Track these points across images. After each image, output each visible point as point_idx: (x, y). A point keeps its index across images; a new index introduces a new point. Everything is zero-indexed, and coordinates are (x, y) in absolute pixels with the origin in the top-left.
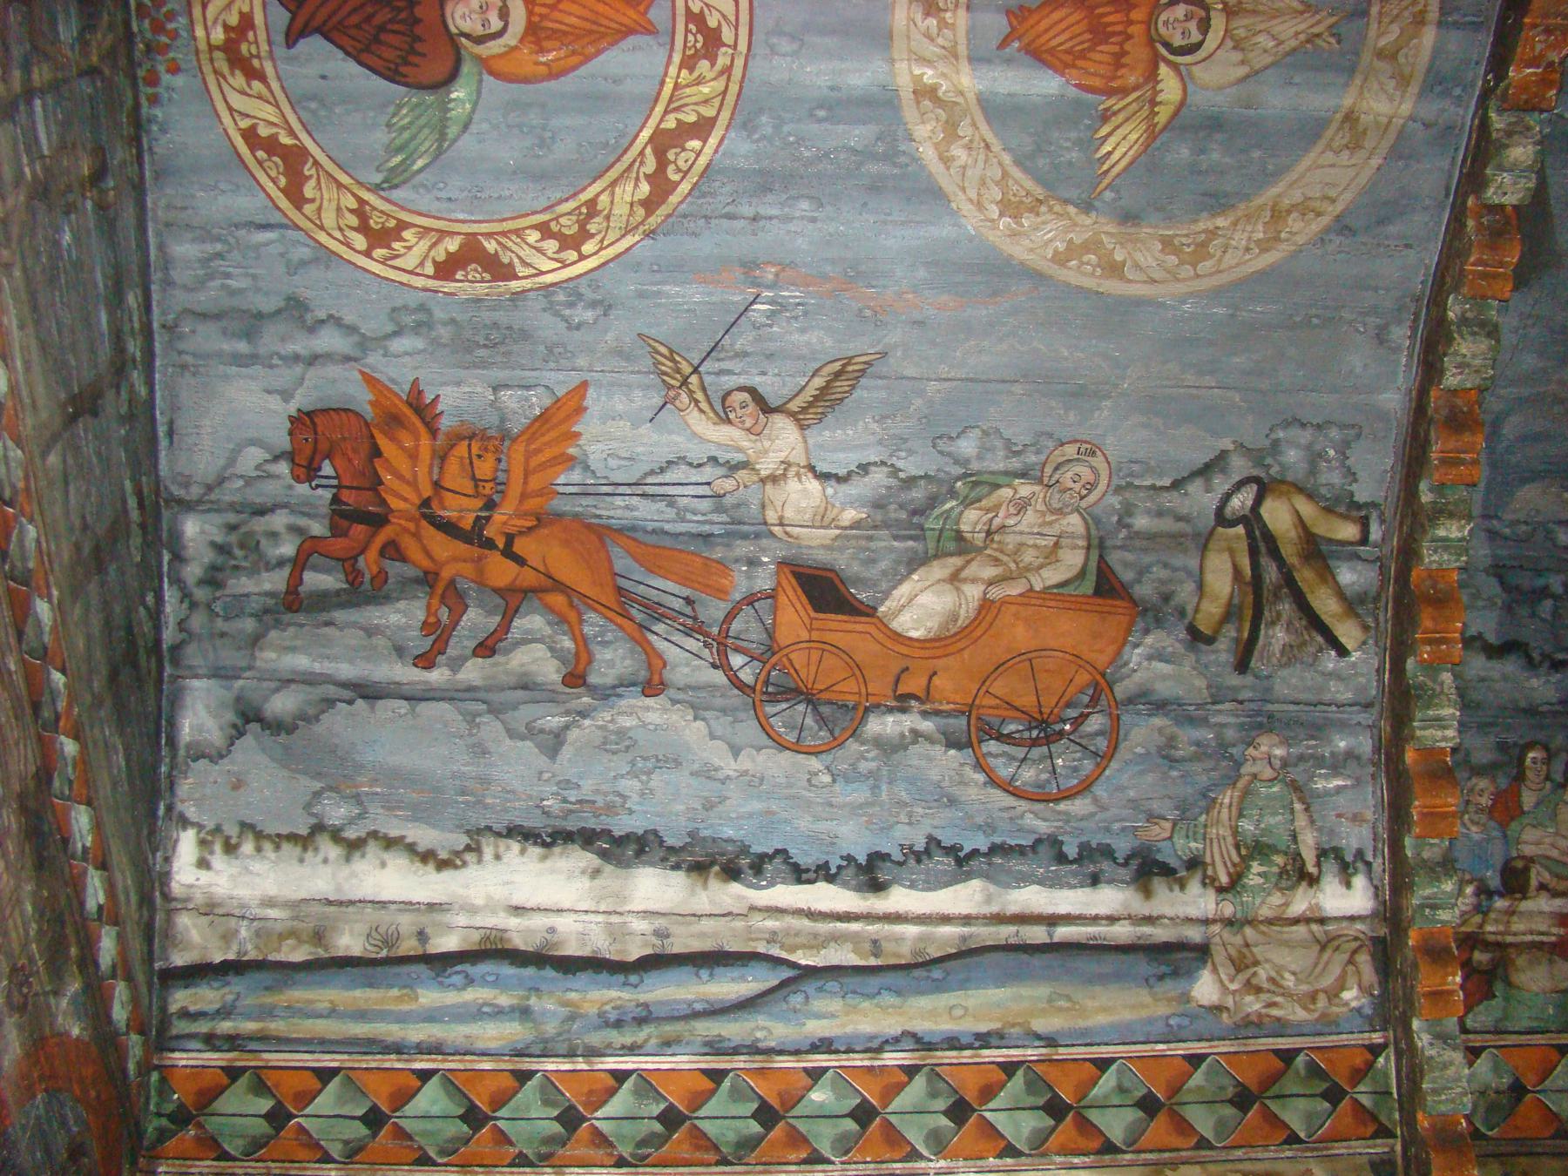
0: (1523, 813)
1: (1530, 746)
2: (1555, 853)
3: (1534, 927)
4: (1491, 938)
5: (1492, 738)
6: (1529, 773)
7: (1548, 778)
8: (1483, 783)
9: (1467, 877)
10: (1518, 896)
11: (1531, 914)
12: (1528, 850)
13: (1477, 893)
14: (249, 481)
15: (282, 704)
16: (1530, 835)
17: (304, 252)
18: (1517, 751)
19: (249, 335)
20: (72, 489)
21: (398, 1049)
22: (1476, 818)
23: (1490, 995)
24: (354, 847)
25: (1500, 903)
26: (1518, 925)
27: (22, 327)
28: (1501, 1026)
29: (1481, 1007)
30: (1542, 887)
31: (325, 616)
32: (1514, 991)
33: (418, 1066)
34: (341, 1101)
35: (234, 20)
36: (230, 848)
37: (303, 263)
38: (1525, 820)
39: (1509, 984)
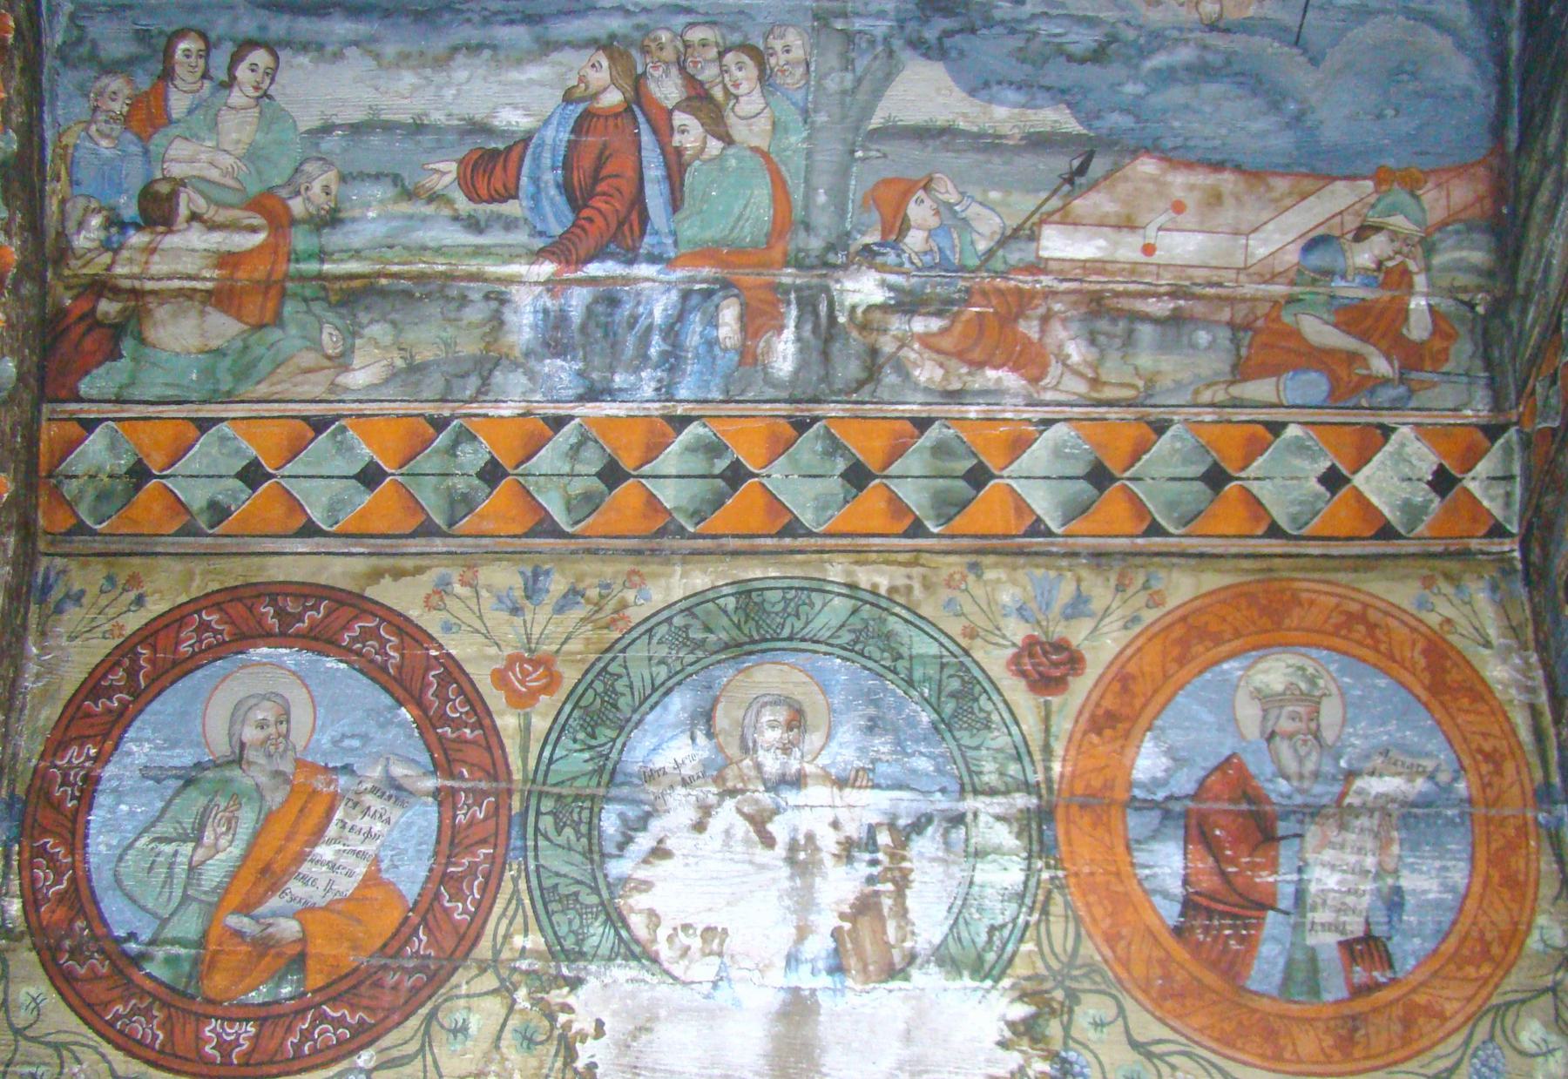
0: (170, 122)
1: (181, 34)
2: (214, 174)
3: (180, 268)
4: (126, 284)
5: (129, 27)
6: (179, 70)
7: (205, 75)
8: (116, 84)
9: (94, 205)
10: (161, 229)
11: (177, 252)
12: (177, 170)
13: (109, 223)
16: (180, 149)
18: (162, 42)
22: (106, 128)
23: (115, 355)
25: (137, 239)
26: (159, 266)
28: (126, 395)
29: (101, 370)
30: (194, 217)
32: (147, 351)
38: (174, 131)
39: (143, 341)
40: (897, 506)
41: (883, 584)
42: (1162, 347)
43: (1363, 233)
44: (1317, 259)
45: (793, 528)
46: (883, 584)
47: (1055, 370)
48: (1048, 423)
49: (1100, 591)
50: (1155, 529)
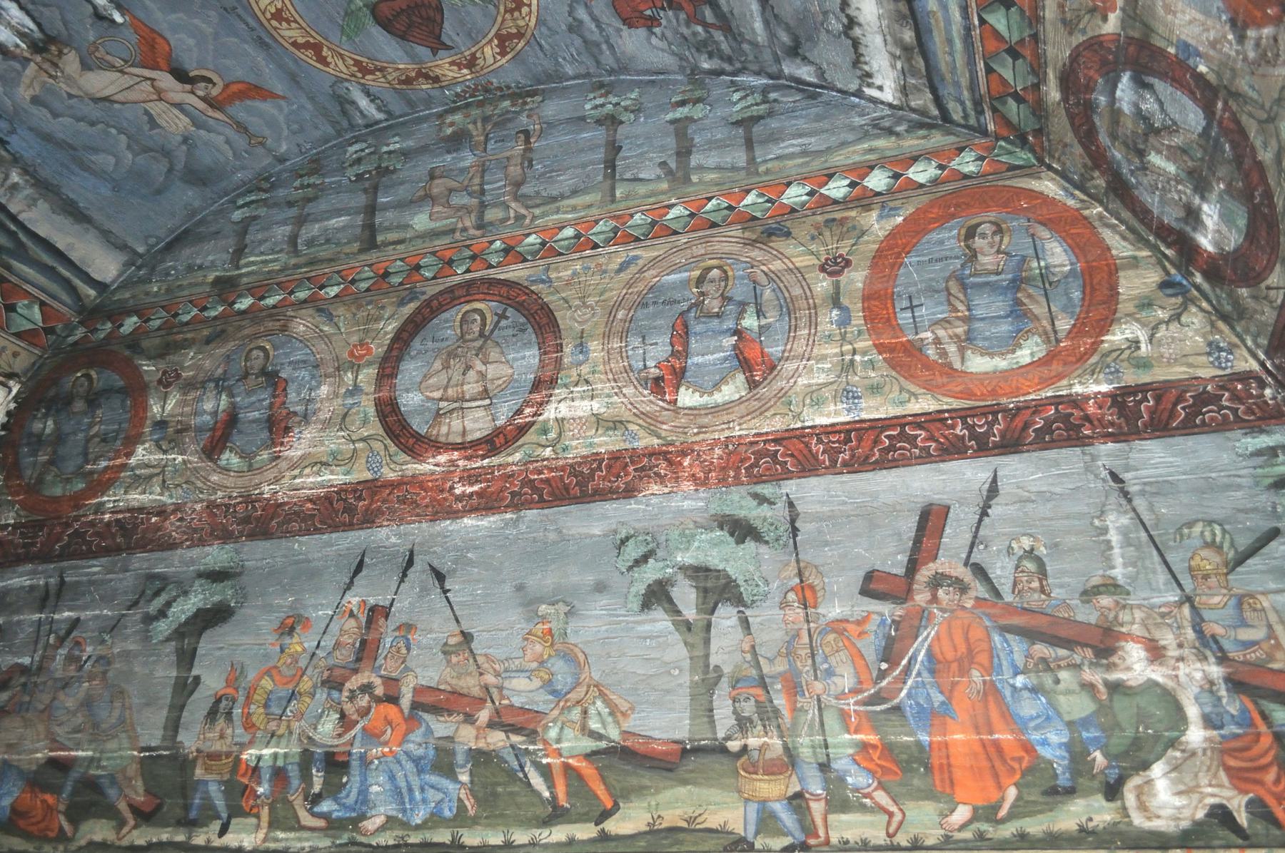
14: (670, 44)
15: (785, 37)
17: (543, 29)
19: (598, 45)
20: (641, 176)
21: (968, 29)
24: (852, 22)
27: (557, 213)
31: (729, 15)
33: (976, 22)
34: (1004, 66)
35: (455, 68)
36: (869, 75)
37: (549, 29)
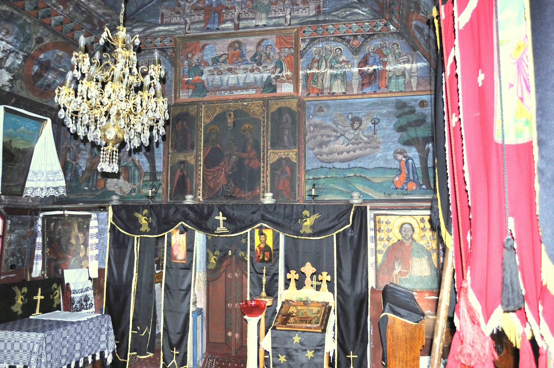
40: (38, 14)
41: (29, 21)
42: (80, 14)
43: (110, 16)
44: (103, 15)
45: (24, 9)
46: (29, 21)
47: (67, 10)
48: (61, 15)
49: (51, 35)
50: (62, 32)
